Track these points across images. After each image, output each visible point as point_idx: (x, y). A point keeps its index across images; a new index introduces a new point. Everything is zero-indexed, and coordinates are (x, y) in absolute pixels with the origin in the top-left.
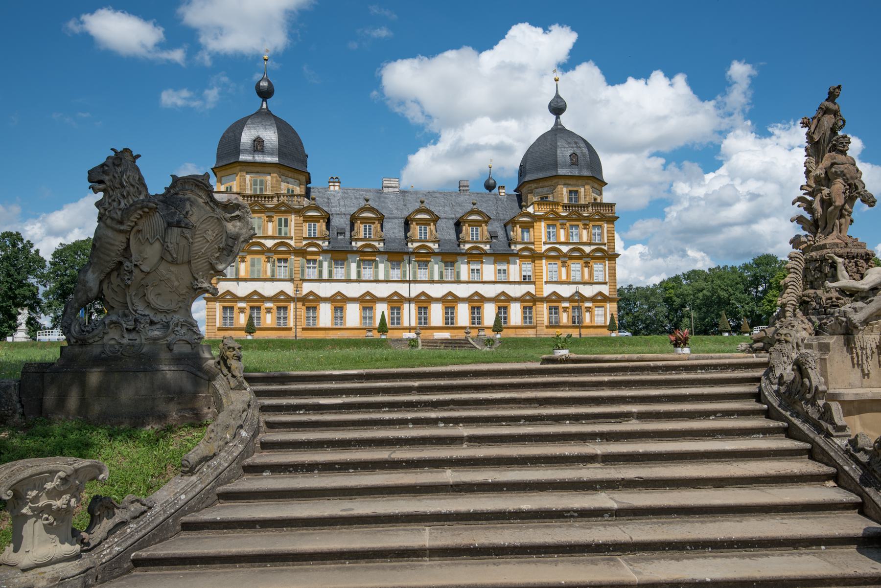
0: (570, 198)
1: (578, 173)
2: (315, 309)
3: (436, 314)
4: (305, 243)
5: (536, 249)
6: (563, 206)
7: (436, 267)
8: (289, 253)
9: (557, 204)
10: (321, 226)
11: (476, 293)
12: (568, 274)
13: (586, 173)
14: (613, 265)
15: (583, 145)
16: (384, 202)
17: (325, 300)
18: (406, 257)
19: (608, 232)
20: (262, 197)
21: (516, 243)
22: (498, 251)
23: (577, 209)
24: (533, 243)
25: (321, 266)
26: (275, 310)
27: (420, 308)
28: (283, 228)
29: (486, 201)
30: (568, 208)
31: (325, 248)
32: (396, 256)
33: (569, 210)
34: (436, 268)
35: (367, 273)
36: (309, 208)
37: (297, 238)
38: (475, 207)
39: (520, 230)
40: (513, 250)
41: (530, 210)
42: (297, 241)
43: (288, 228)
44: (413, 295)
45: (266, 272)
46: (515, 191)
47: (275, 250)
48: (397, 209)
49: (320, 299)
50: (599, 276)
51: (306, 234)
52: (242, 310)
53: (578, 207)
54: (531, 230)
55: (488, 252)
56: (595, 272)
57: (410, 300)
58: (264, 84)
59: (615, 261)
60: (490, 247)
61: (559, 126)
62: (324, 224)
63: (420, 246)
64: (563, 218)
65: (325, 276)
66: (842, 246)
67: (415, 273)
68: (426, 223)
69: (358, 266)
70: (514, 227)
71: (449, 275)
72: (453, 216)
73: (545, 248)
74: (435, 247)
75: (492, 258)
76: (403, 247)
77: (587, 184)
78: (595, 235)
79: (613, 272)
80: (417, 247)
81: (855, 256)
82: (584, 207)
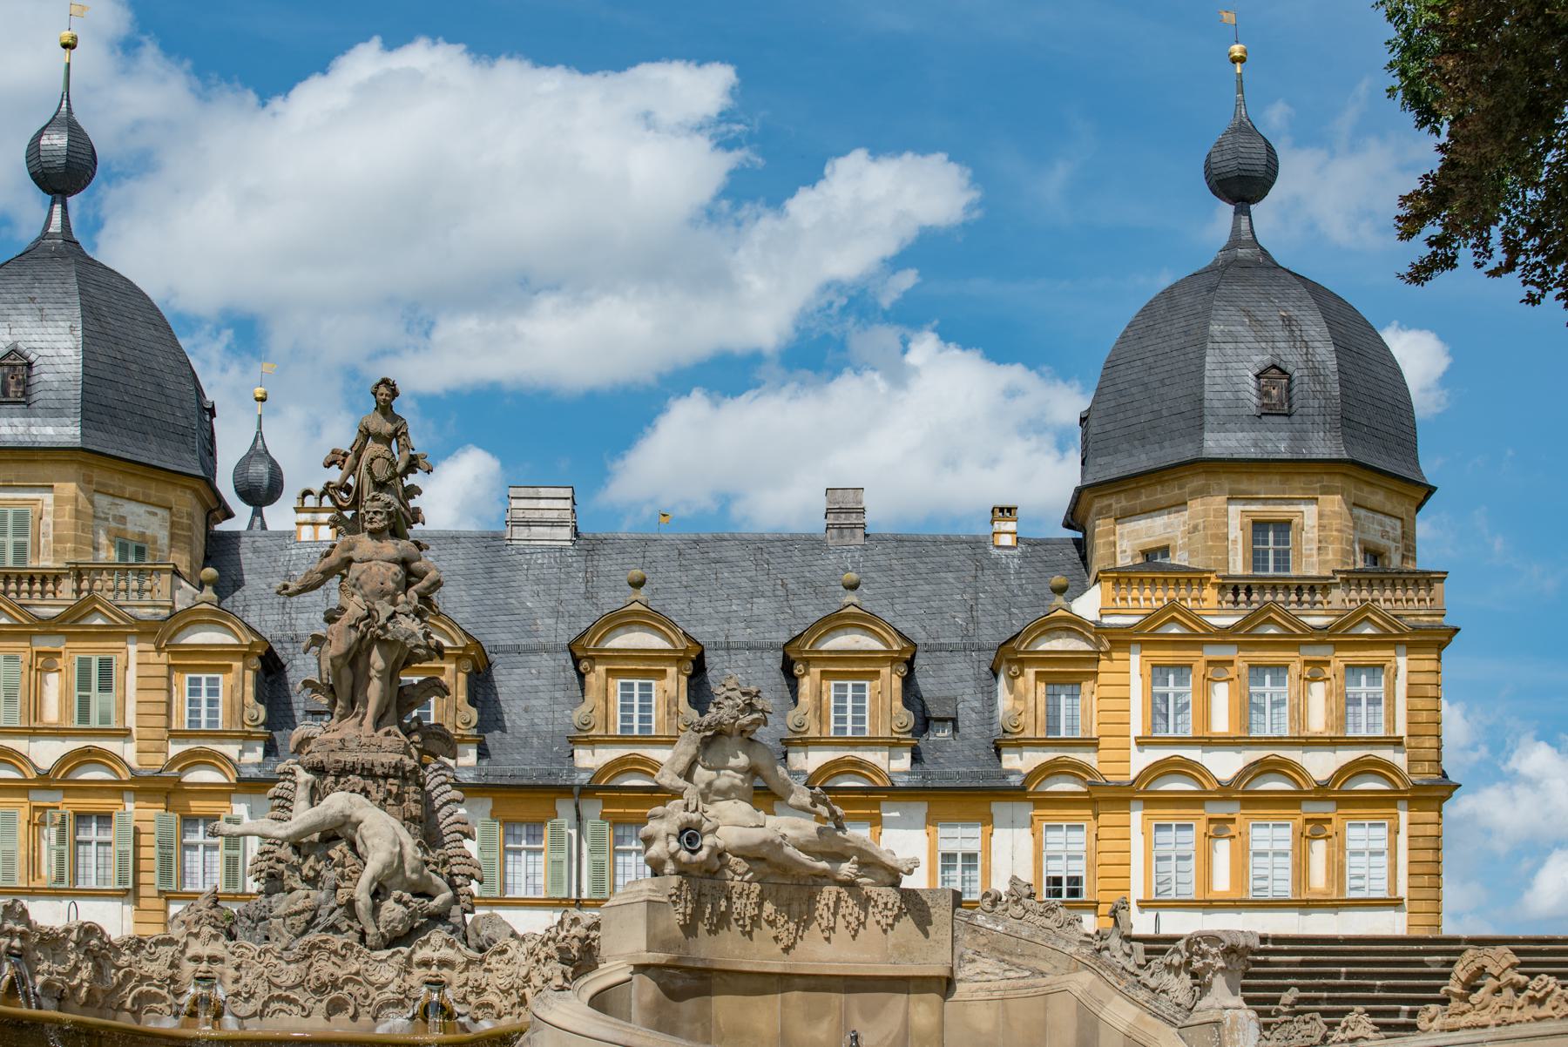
0: (1255, 552)
1: (1291, 449)
4: (175, 749)
5: (1103, 768)
6: (1222, 588)
9: (1192, 578)
12: (1239, 870)
13: (1323, 446)
14: (1431, 830)
15: (1315, 328)
16: (506, 585)
18: (565, 809)
19: (1413, 691)
20: (19, 580)
21: (1020, 745)
22: (943, 776)
23: (1280, 597)
24: (1091, 744)
28: (95, 695)
29: (934, 571)
30: (1242, 597)
31: (253, 772)
33: (1249, 602)
37: (147, 733)
38: (851, 597)
39: (1042, 687)
40: (1012, 772)
41: (1088, 605)
42: (145, 745)
43: (112, 698)
45: (33, 864)
46: (1068, 525)
47: (63, 780)
48: (557, 614)
50: (1370, 877)
51: (181, 721)
53: (1287, 588)
54: (1087, 686)
55: (901, 782)
56: (1351, 861)
59: (1439, 811)
60: (916, 758)
61: (1241, 252)
62: (250, 675)
63: (621, 761)
64: (1223, 636)
66: (333, 746)
68: (646, 665)
70: (1013, 678)
73: (1141, 760)
75: (920, 809)
76: (555, 767)
77: (1327, 491)
78: (1357, 702)
79: (1430, 855)
80: (609, 767)
82: (1312, 590)
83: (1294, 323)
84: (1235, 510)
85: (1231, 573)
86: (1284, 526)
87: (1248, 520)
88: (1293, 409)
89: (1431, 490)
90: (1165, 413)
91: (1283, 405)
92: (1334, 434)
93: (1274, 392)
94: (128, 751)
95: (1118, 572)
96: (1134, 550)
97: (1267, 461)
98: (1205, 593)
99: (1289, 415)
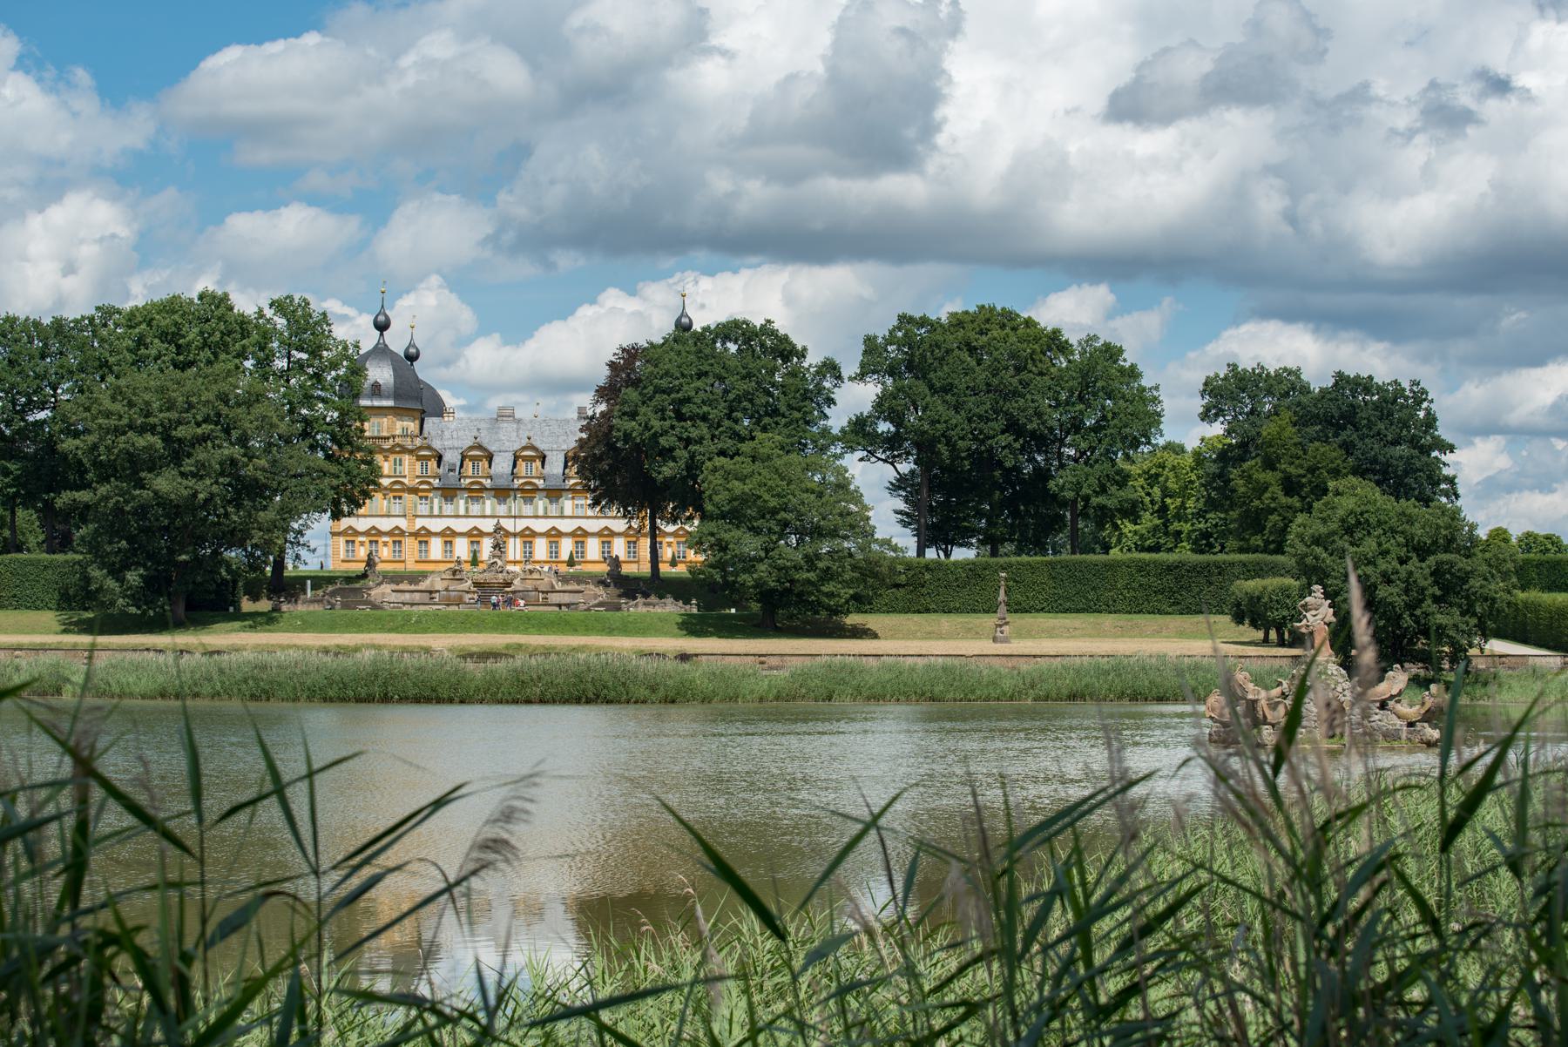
2: (426, 542)
3: (541, 549)
7: (541, 503)
8: (403, 490)
10: (433, 464)
11: (580, 528)
17: (436, 534)
18: (512, 493)
25: (432, 503)
26: (391, 544)
27: (525, 542)
32: (502, 493)
34: (541, 504)
35: (475, 508)
36: (421, 448)
44: (518, 530)
49: (430, 533)
51: (418, 473)
52: (362, 544)
57: (515, 535)
58: (381, 318)
65: (436, 512)
67: (520, 510)
68: (531, 459)
69: (467, 503)
71: (553, 509)
72: (564, 447)
74: (540, 483)
94: (406, 481)
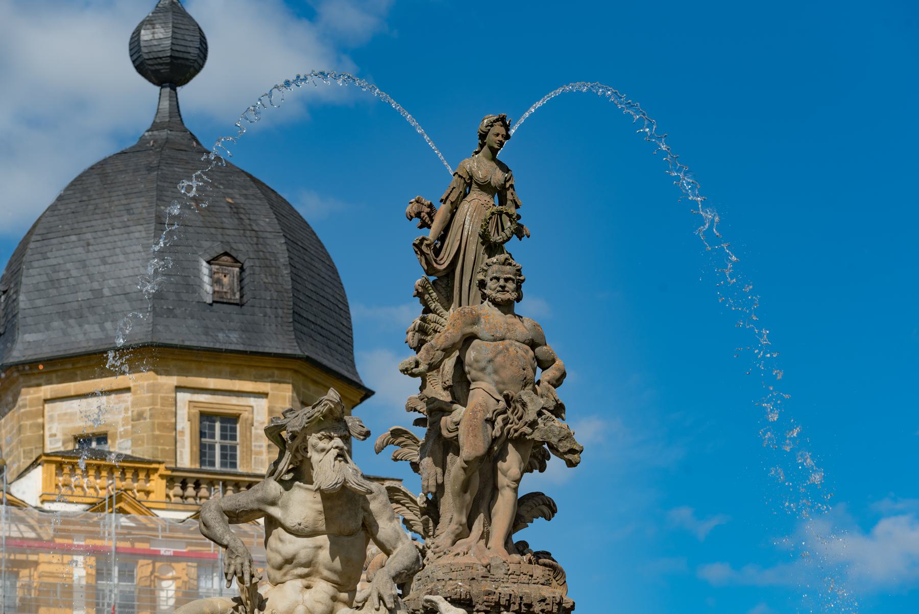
0: (202, 446)
6: (171, 481)
30: (190, 491)
66: (474, 573)
81: (503, 602)
83: (242, 211)
84: (183, 397)
85: (179, 466)
86: (230, 420)
87: (196, 411)
88: (245, 299)
89: (369, 393)
90: (106, 292)
91: (234, 294)
92: (286, 328)
93: (226, 280)
95: (63, 457)
96: (65, 434)
97: (220, 351)
98: (149, 486)
99: (240, 305)
